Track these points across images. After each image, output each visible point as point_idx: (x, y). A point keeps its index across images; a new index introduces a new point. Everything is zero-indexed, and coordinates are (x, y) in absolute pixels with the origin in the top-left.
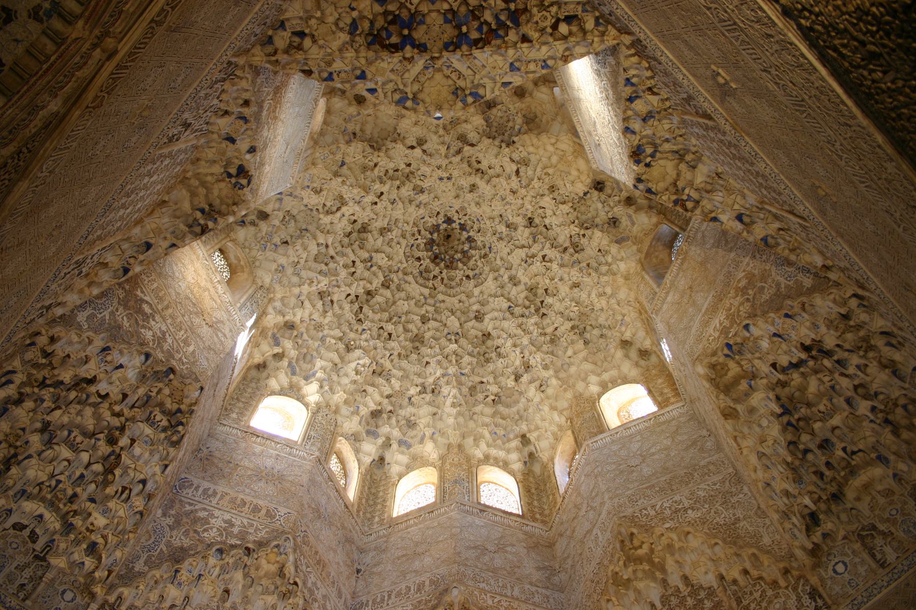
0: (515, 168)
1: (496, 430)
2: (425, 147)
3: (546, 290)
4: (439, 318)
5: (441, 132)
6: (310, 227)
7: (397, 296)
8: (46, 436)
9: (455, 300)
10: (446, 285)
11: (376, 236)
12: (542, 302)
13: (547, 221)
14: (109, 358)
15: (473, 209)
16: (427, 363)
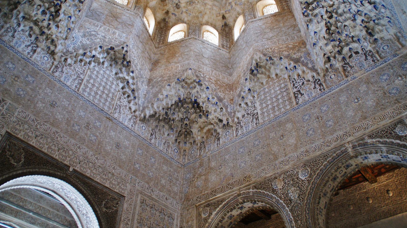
14: (316, 41)
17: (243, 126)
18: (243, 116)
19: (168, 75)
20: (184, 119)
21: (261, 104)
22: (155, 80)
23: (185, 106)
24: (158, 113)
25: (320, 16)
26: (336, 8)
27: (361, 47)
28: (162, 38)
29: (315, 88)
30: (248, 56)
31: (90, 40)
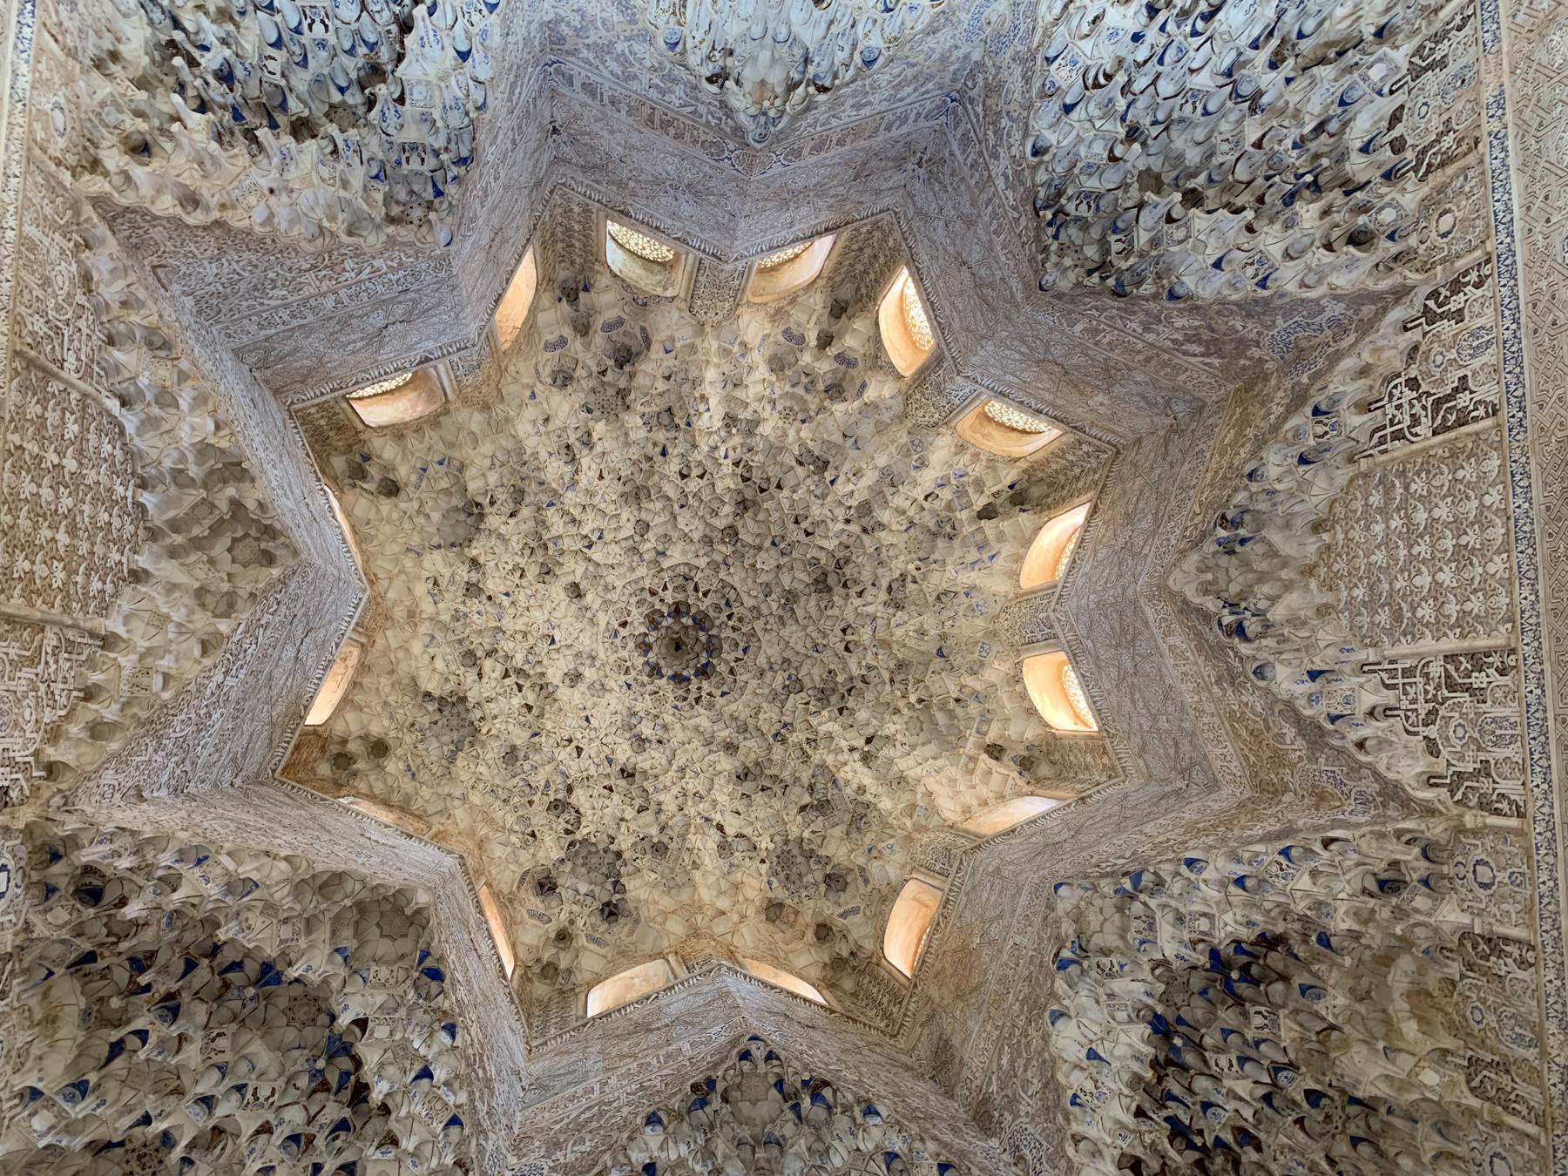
0: (730, 831)
1: (443, 468)
2: (856, 755)
3: (529, 708)
4: (623, 544)
5: (868, 797)
6: (905, 536)
7: (701, 527)
8: (1246, 89)
9: (619, 584)
10: (642, 589)
11: (795, 584)
12: (520, 688)
13: (616, 798)
14: (1250, 271)
15: (702, 718)
16: (601, 477)
17: (1482, 756)
18: (1432, 748)
19: (1017, 1007)
20: (1274, 1084)
21: (1412, 633)
22: (994, 1087)
23: (1208, 1041)
24: (1139, 1152)
25: (1166, 227)
26: (1174, 174)
27: (1380, 93)
28: (885, 1001)
29: (1459, 316)
30: (1171, 641)
31: (588, 1137)
